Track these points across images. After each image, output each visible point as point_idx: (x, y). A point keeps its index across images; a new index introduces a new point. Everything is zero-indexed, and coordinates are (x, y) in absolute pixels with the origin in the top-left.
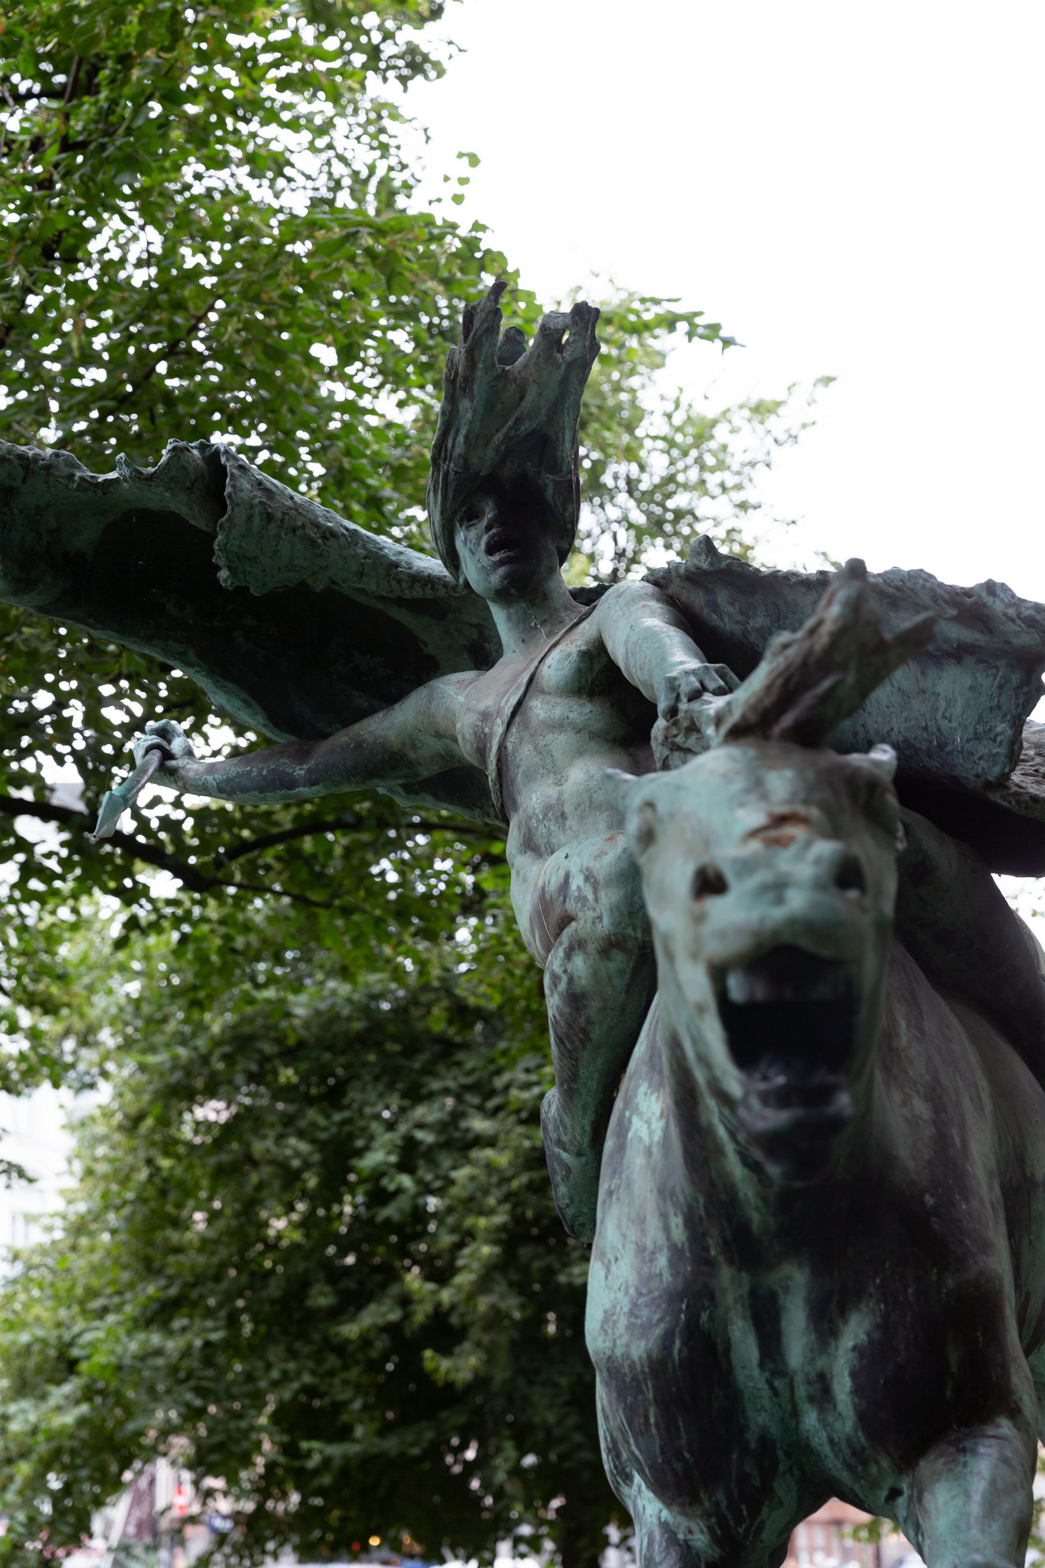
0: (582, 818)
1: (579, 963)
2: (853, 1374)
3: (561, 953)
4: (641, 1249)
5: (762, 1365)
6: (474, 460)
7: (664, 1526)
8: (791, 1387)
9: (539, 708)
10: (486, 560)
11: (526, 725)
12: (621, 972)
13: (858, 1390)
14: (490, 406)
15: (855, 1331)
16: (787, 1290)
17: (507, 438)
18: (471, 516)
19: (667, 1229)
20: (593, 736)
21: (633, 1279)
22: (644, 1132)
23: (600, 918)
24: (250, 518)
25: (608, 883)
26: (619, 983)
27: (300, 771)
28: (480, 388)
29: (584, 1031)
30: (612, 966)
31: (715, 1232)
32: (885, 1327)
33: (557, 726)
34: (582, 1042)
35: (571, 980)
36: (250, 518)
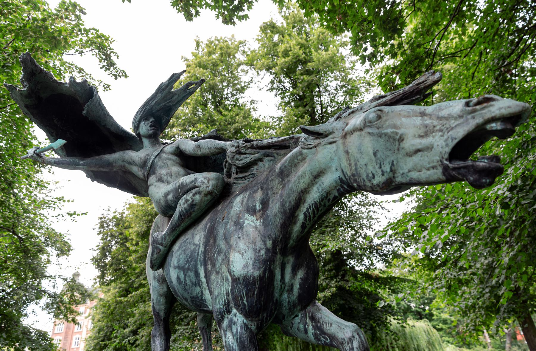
0: (176, 177)
1: (197, 197)
2: (300, 284)
3: (191, 194)
4: (255, 250)
5: (281, 281)
6: (154, 108)
7: (245, 324)
8: (285, 287)
9: (164, 155)
10: (149, 128)
11: (160, 158)
12: (208, 200)
13: (300, 289)
14: (164, 98)
15: (300, 274)
16: (288, 263)
17: (165, 105)
18: (146, 119)
19: (265, 244)
20: (177, 163)
21: (253, 256)
22: (252, 223)
23: (209, 187)
24: (96, 102)
25: (213, 180)
26: (206, 203)
27: (82, 162)
28: (165, 92)
29: (191, 214)
30: (206, 198)
31: (280, 245)
32: (307, 273)
33: (170, 159)
34: (188, 216)
35: (193, 201)
36: (96, 102)
